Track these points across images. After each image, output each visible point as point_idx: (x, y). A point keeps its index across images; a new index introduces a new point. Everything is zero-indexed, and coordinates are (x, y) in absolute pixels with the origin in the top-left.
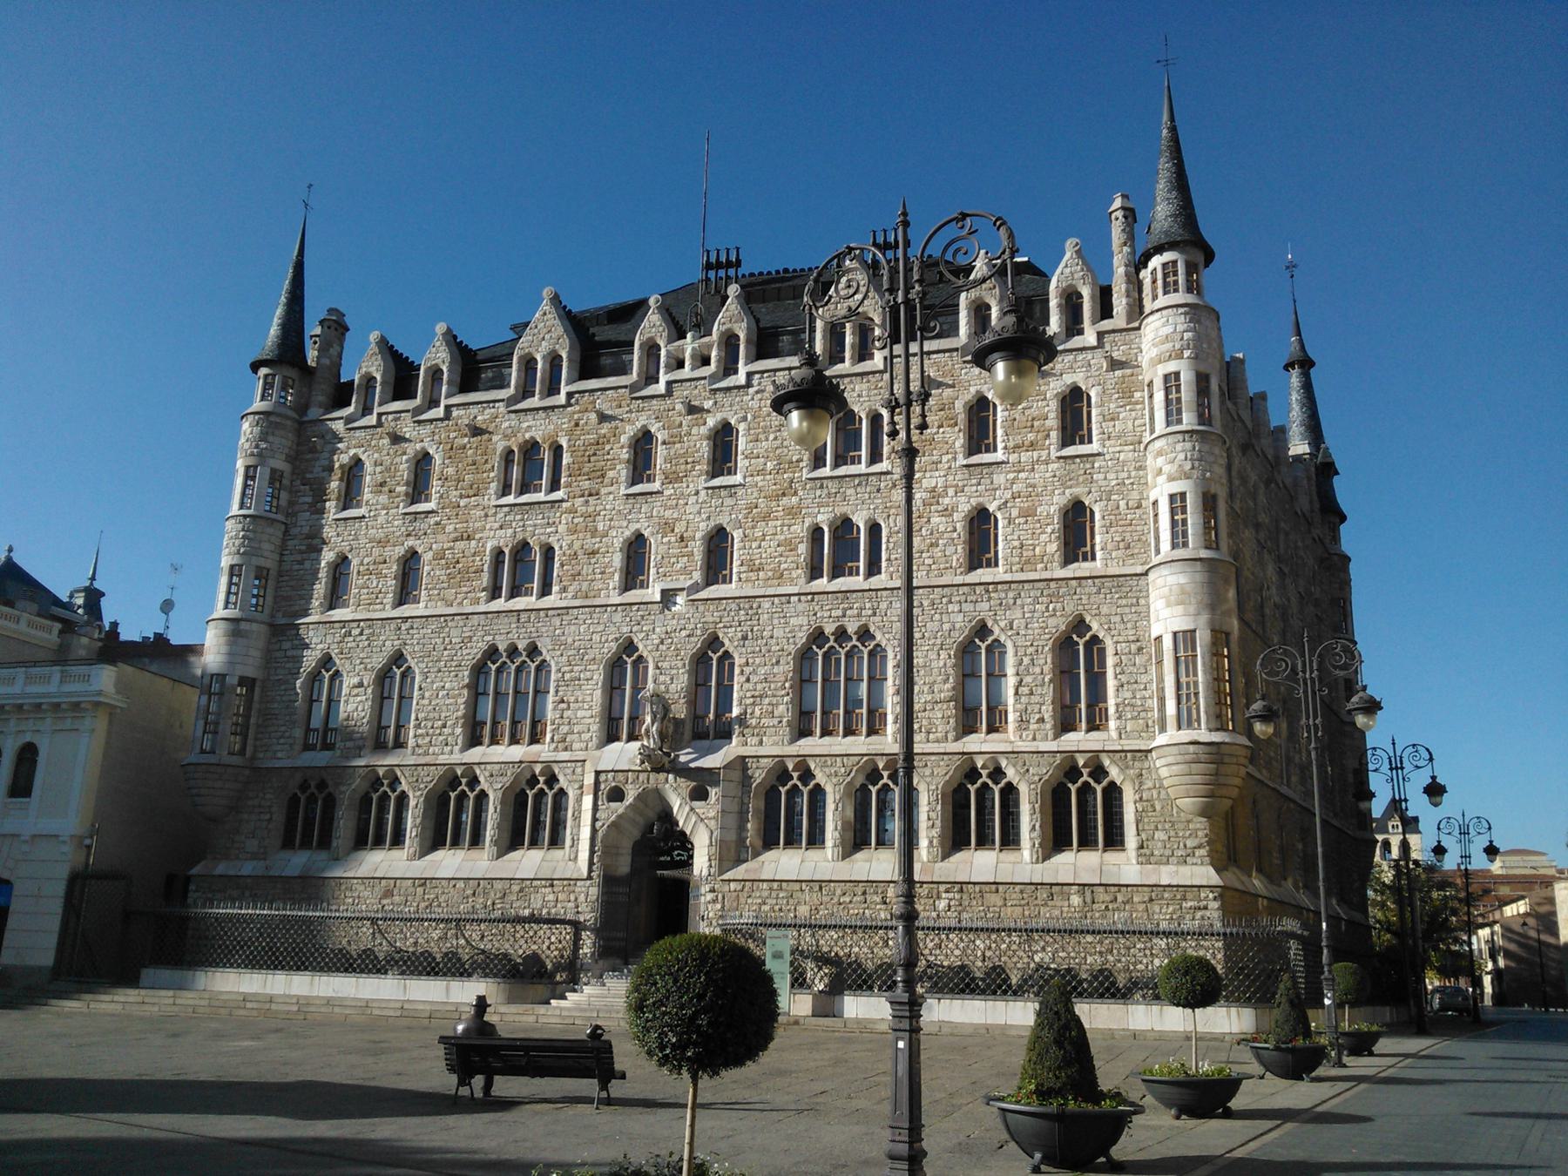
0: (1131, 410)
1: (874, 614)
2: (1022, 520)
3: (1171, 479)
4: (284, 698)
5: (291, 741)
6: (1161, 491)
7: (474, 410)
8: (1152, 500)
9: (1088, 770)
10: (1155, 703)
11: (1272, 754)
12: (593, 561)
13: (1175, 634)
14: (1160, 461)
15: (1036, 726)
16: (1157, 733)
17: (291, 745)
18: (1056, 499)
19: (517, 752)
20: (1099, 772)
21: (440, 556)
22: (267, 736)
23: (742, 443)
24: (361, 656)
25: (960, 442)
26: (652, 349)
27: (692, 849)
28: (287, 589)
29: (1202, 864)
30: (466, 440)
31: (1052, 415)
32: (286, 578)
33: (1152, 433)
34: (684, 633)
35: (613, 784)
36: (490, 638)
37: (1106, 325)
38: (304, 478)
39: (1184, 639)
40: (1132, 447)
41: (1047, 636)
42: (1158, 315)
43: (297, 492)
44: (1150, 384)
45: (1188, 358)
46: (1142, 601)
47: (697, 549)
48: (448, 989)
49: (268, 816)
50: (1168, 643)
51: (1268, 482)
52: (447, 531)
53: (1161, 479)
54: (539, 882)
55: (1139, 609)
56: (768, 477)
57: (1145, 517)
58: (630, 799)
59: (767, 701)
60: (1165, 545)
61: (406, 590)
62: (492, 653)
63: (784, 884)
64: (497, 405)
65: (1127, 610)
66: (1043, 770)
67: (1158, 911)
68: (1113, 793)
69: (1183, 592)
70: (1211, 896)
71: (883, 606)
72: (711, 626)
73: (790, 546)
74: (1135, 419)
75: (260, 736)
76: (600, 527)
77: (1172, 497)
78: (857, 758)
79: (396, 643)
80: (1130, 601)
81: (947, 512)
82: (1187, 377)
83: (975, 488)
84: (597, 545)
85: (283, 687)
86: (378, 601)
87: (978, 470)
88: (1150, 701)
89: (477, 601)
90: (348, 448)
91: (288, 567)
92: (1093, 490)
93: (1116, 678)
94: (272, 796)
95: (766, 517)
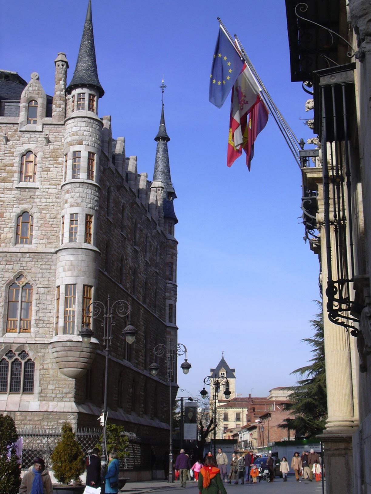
0: (56, 167)
3: (72, 206)
6: (67, 211)
8: (62, 215)
9: (18, 352)
10: (54, 320)
11: (119, 344)
13: (67, 285)
14: (67, 196)
16: (54, 335)
18: (14, 209)
20: (23, 354)
29: (70, 401)
33: (65, 181)
37: (48, 120)
40: (55, 187)
41: (3, 282)
42: (72, 120)
44: (66, 155)
45: (85, 145)
46: (53, 267)
50: (62, 289)
51: (132, 205)
53: (67, 205)
55: (51, 271)
57: (58, 223)
60: (66, 240)
65: (45, 271)
67: (46, 424)
68: (30, 365)
69: (72, 265)
70: (72, 417)
74: (58, 172)
82: (84, 155)
88: (52, 318)
92: (34, 207)
93: (36, 306)
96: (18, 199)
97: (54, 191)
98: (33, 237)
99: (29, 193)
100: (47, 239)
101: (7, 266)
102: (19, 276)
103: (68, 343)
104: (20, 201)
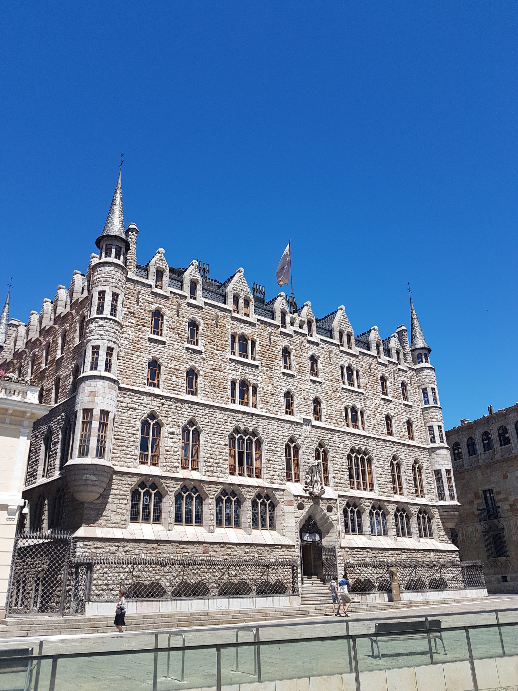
5: (134, 457)
7: (217, 311)
16: (438, 500)
19: (253, 481)
22: (118, 452)
23: (320, 366)
24: (173, 417)
28: (123, 367)
32: (124, 362)
35: (300, 502)
36: (236, 423)
47: (310, 403)
58: (306, 509)
59: (341, 473)
61: (192, 389)
62: (237, 430)
64: (227, 311)
72: (321, 438)
75: (115, 451)
76: (275, 383)
79: (191, 414)
83: (386, 407)
84: (275, 391)
85: (127, 424)
95: (331, 398)
99: (409, 408)
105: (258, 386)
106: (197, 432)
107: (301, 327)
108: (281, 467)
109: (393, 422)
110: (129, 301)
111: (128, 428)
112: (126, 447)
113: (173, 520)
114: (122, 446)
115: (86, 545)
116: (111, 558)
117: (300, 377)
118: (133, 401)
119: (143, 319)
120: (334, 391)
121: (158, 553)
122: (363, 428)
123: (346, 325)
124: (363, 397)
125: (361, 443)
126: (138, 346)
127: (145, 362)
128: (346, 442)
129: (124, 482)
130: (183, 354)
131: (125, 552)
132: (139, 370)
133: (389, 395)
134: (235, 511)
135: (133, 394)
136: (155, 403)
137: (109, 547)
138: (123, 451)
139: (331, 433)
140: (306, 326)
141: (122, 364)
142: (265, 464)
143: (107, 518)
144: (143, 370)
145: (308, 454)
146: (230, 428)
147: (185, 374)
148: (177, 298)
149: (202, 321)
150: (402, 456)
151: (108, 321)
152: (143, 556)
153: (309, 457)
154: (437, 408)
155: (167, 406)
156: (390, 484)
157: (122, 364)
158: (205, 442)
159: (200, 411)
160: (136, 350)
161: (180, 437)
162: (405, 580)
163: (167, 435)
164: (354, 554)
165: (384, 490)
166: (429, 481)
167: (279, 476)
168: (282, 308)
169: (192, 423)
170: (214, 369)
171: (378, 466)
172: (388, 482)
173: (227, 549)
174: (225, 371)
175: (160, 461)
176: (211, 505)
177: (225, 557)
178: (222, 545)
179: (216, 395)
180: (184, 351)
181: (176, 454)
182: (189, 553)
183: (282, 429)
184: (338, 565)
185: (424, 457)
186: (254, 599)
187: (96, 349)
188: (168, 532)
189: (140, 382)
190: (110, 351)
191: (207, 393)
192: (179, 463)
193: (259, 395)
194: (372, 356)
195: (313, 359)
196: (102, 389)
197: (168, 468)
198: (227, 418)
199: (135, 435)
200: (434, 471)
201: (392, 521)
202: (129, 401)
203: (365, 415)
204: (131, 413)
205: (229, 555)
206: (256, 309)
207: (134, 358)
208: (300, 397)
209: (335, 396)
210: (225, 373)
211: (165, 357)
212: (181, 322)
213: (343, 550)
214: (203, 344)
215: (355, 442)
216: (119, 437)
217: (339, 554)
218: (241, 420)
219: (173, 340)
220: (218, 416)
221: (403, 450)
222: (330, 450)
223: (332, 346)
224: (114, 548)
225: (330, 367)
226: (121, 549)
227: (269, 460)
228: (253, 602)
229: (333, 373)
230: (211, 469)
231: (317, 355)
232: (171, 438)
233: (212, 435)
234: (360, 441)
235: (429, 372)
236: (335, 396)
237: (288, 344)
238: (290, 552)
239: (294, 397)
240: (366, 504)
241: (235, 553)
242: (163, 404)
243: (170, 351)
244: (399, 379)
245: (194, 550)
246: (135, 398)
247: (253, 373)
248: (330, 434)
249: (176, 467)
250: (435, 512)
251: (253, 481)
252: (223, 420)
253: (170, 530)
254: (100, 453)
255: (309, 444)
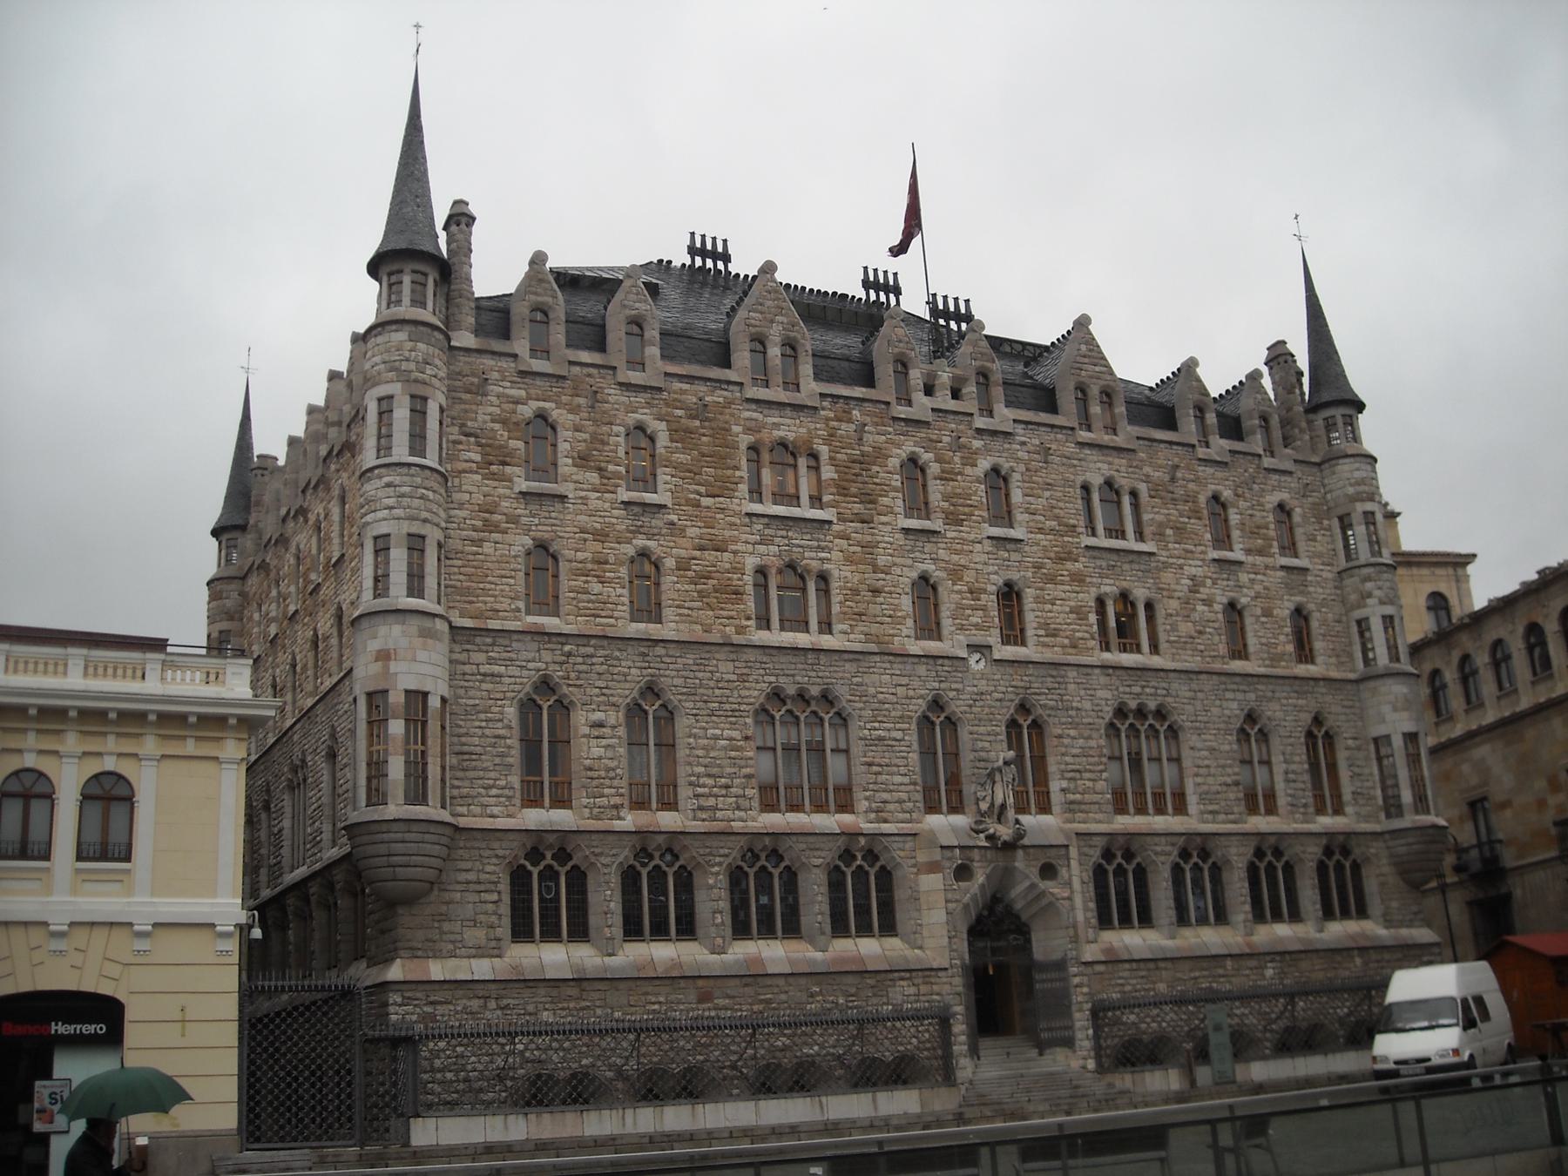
1: (1168, 695)
2: (1263, 619)
3: (1382, 603)
4: (487, 732)
5: (506, 792)
7: (702, 388)
10: (1379, 792)
12: (882, 600)
14: (1369, 585)
15: (1302, 810)
16: (1382, 815)
17: (509, 798)
19: (828, 822)
21: (683, 566)
22: (467, 783)
23: (1017, 496)
25: (1208, 536)
26: (902, 365)
27: (1029, 933)
28: (461, 577)
30: (697, 423)
31: (1272, 526)
32: (459, 563)
33: (1348, 557)
34: (996, 695)
36: (773, 679)
38: (463, 425)
39: (1411, 738)
42: (1352, 460)
43: (455, 442)
47: (990, 600)
48: (874, 1100)
49: (495, 897)
50: (1398, 742)
52: (688, 534)
53: (1369, 601)
54: (896, 975)
55: (1358, 711)
56: (1049, 537)
58: (980, 878)
59: (1087, 775)
62: (777, 695)
63: (1142, 965)
64: (731, 388)
65: (1348, 711)
66: (1313, 851)
71: (1175, 686)
72: (1021, 691)
73: (1079, 612)
75: (456, 783)
76: (882, 560)
77: (1384, 617)
78: (1175, 839)
79: (645, 672)
80: (1350, 703)
81: (1208, 602)
83: (1225, 583)
84: (882, 582)
85: (483, 716)
86: (603, 613)
87: (1227, 566)
89: (741, 630)
90: (529, 398)
91: (460, 548)
94: (497, 869)
95: (1052, 579)
96: (1287, 585)
97: (1330, 576)
98: (1316, 653)
100: (1338, 656)
101: (1300, 702)
102: (1318, 720)
103: (1431, 831)
104: (1289, 588)
105: (830, 575)
106: (668, 715)
107: (956, 394)
108: (906, 780)
109: (1248, 621)
110: (463, 406)
111: (484, 724)
112: (484, 769)
113: (618, 931)
114: (474, 769)
115: (409, 998)
116: (470, 1025)
117: (954, 534)
118: (490, 658)
119: (501, 447)
120: (1061, 559)
121: (583, 1009)
122: (1155, 648)
123: (1097, 369)
124: (1153, 564)
125: (1148, 690)
126: (497, 517)
127: (515, 557)
128: (1100, 693)
129: (487, 853)
130: (614, 521)
131: (502, 1009)
132: (502, 577)
133: (1237, 547)
134: (782, 899)
135: (489, 640)
136: (547, 656)
137: (464, 1001)
138: (480, 782)
139: (1054, 673)
140: (970, 389)
141: (456, 570)
142: (861, 775)
143: (452, 937)
144: (511, 577)
145: (984, 738)
146: (756, 693)
147: (624, 572)
148: (589, 375)
149: (663, 426)
150: (1273, 711)
151: (405, 470)
152: (546, 1016)
153: (987, 745)
154: (1378, 568)
155: (580, 660)
156: (1235, 789)
157: (456, 570)
158: (690, 737)
159: (668, 660)
160: (490, 527)
161: (622, 731)
162: (1272, 1031)
163: (586, 730)
164: (1120, 978)
165: (1215, 807)
166: (1356, 770)
167: (900, 802)
168: (896, 350)
169: (651, 690)
170: (702, 548)
171: (1199, 745)
172: (1228, 785)
173: (760, 990)
174: (734, 547)
175: (575, 794)
176: (715, 891)
177: (755, 1008)
178: (745, 980)
179: (711, 613)
180: (615, 512)
181: (612, 774)
182: (660, 1003)
183: (904, 681)
184: (1074, 1008)
185: (1344, 707)
186: (824, 1099)
187: (382, 546)
188: (606, 959)
189: (505, 606)
190: (416, 544)
191: (686, 611)
192: (622, 795)
193: (836, 598)
194: (1178, 444)
195: (997, 478)
196: (404, 642)
197: (596, 811)
198: (745, 671)
199: (505, 738)
200: (1376, 740)
201: (1238, 885)
202: (481, 657)
203: (1160, 614)
204: (489, 686)
205: (768, 1002)
206: (821, 362)
207: (486, 550)
208: (957, 588)
209: (1065, 573)
210: (735, 553)
211: (567, 535)
212: (605, 438)
213: (1089, 970)
214: (668, 486)
215: (1128, 689)
216: (466, 748)
217: (1076, 980)
218: (786, 672)
219: (585, 486)
220: (722, 667)
221: (1277, 695)
222: (1051, 720)
223: (1052, 435)
224: (475, 1004)
225: (1047, 494)
226: (492, 1004)
227: (870, 764)
228: (822, 1108)
229: (1057, 511)
230: (711, 802)
231: (1007, 465)
232: (597, 738)
233: (706, 718)
234: (1143, 687)
235: (1358, 469)
236: (1065, 573)
237: (914, 449)
238: (935, 987)
239: (940, 589)
240: (1159, 849)
241: (783, 997)
242: (569, 654)
243: (579, 517)
244: (1268, 498)
245: (672, 997)
246: (496, 649)
247: (815, 543)
248: (1053, 676)
249: (616, 807)
250: (1373, 851)
251: (828, 822)
252: (734, 677)
253: (610, 955)
254: (417, 794)
255: (987, 710)
